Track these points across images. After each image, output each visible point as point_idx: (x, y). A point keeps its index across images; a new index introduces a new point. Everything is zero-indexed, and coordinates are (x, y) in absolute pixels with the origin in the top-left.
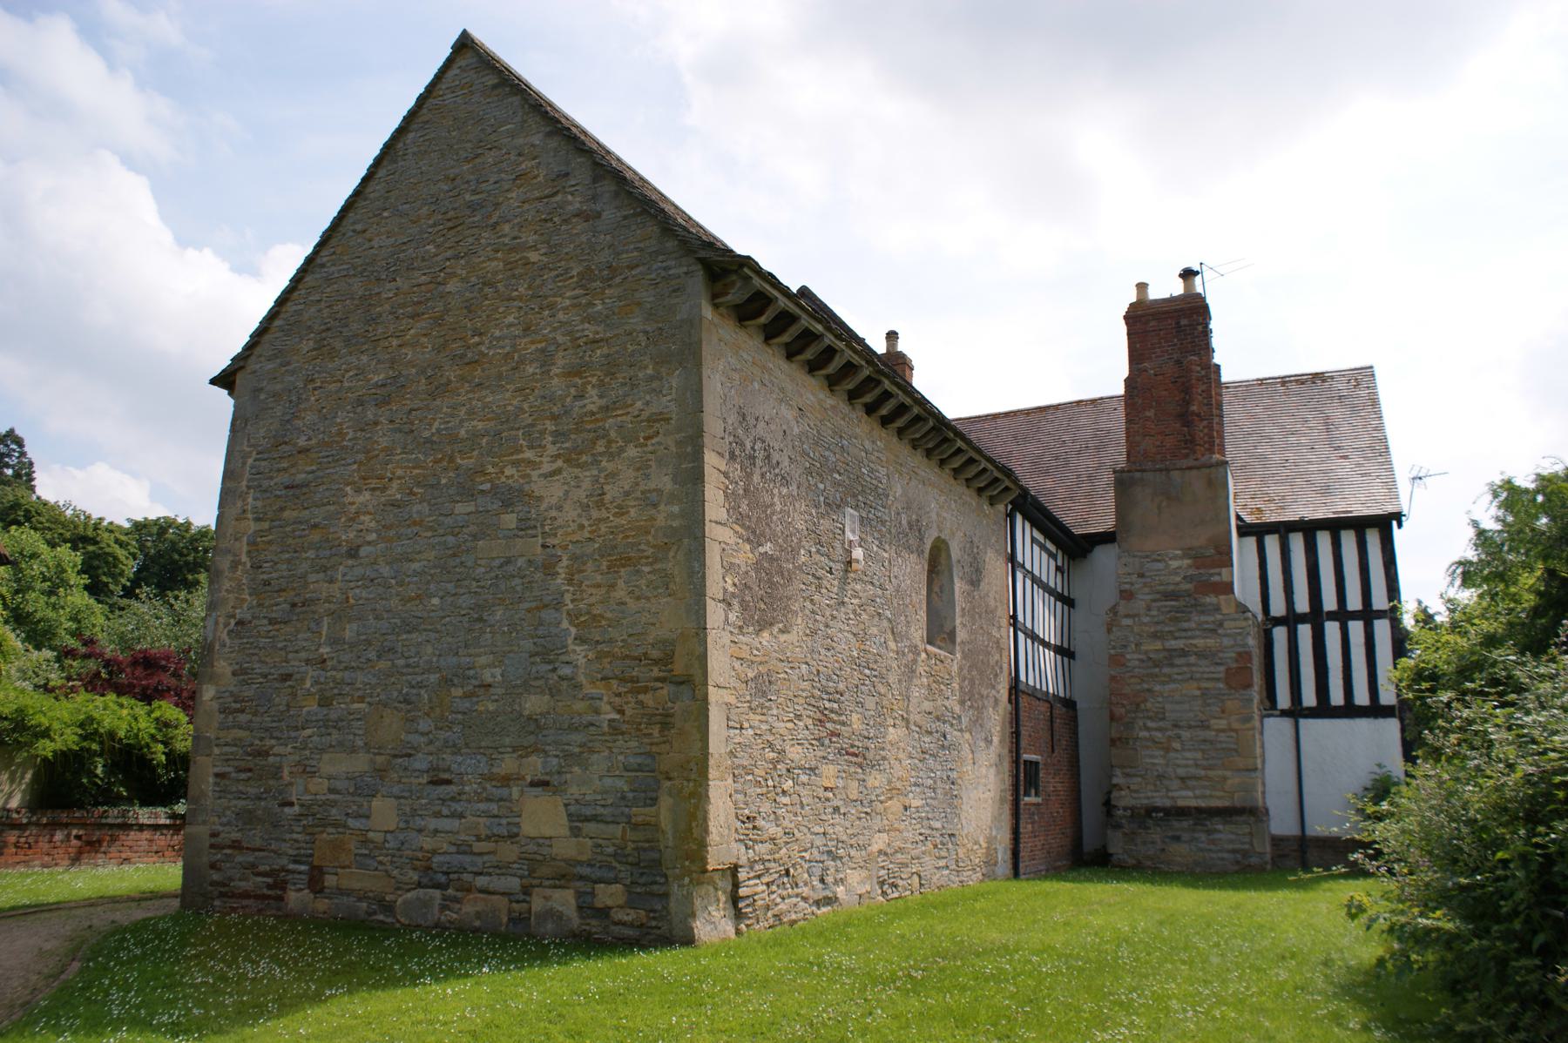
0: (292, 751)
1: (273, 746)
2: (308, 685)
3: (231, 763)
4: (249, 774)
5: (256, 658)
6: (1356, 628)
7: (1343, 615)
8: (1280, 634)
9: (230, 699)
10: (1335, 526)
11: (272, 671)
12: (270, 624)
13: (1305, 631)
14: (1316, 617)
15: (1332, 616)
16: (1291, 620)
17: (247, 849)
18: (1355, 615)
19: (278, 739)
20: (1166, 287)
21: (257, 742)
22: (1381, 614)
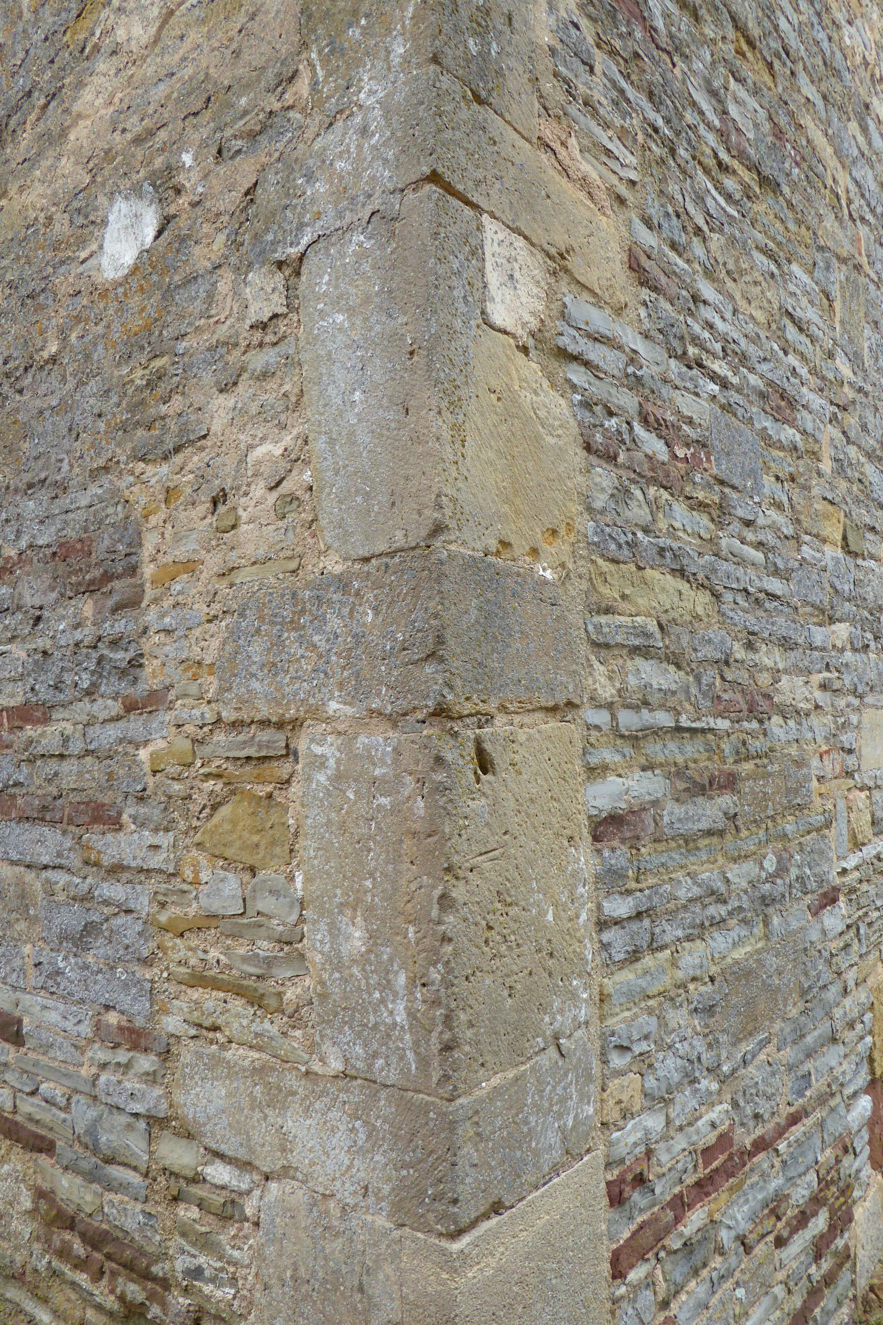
0: (818, 694)
1: (776, 674)
2: (826, 466)
3: (654, 749)
4: (726, 800)
5: (698, 249)
9: (627, 401)
11: (752, 350)
12: (722, 134)
17: (761, 1145)
19: (786, 644)
21: (740, 653)
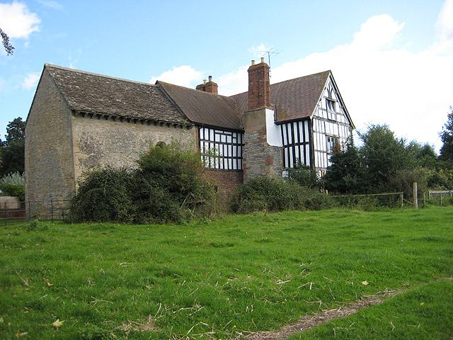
6: (302, 147)
7: (299, 144)
8: (286, 149)
10: (297, 121)
13: (291, 148)
14: (293, 145)
15: (297, 144)
16: (288, 146)
18: (302, 144)
20: (257, 63)
22: (307, 143)
